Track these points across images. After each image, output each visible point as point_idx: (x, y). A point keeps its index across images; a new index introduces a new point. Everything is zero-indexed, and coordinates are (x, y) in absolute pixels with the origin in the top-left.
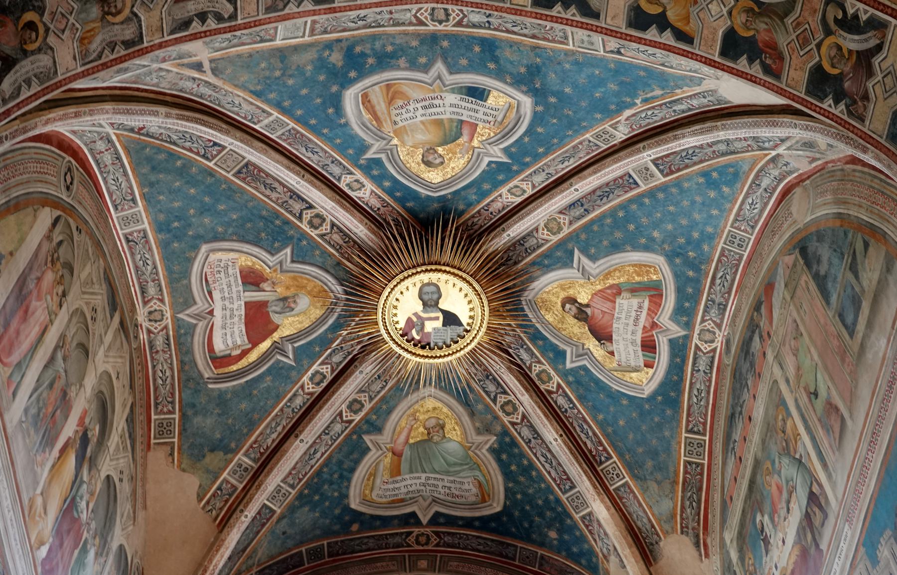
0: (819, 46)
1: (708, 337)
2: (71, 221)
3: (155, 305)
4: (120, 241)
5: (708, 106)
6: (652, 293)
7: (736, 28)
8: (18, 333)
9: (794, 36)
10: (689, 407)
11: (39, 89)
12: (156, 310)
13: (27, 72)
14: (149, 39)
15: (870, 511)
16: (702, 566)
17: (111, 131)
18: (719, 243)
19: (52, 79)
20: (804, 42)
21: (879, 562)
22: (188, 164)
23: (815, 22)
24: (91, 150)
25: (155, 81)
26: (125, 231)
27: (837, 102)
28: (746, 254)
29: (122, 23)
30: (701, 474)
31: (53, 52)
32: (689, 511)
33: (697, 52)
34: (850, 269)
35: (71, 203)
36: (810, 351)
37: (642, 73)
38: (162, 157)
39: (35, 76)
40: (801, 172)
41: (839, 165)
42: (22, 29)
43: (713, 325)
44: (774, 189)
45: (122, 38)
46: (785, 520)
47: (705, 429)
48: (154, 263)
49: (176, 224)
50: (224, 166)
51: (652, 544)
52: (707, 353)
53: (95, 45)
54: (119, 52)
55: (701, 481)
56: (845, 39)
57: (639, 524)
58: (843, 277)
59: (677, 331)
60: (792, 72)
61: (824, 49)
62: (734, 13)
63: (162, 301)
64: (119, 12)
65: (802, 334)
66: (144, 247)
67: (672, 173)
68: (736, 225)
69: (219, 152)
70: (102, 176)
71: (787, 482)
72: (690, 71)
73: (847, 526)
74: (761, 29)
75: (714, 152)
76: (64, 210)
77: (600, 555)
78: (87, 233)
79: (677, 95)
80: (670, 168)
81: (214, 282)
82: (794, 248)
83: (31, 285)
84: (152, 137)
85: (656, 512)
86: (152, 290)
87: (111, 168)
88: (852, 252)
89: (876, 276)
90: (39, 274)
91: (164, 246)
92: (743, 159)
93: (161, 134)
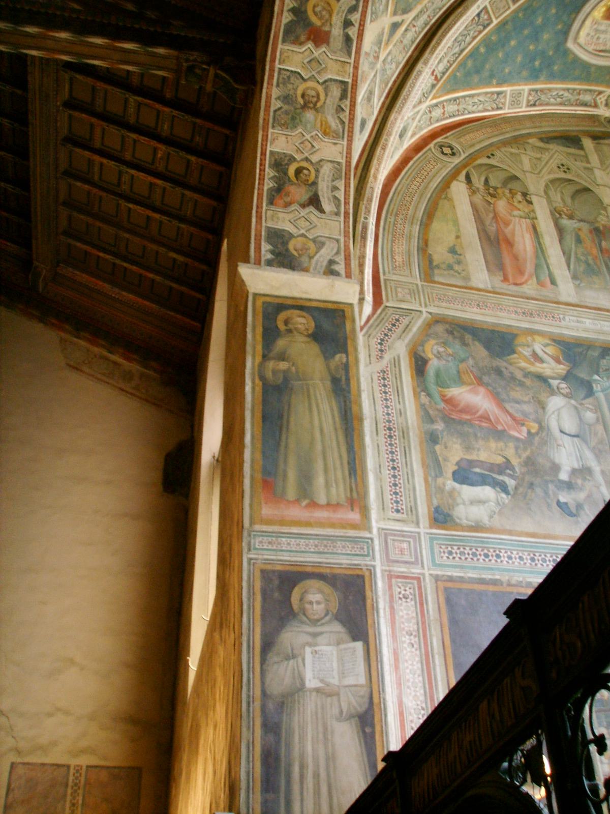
2: (479, 161)
3: (601, 99)
4: (530, 111)
8: (516, 258)
11: (343, 181)
12: (606, 100)
13: (328, 187)
14: (347, 76)
17: (428, 103)
19: (341, 169)
22: (486, 42)
24: (438, 121)
25: (394, 66)
26: (524, 105)
29: (327, 95)
31: (324, 160)
35: (466, 154)
38: (470, 63)
39: (333, 181)
42: (297, 179)
45: (337, 100)
48: (564, 90)
49: (537, 63)
50: (501, 12)
53: (334, 123)
54: (346, 106)
63: (600, 93)
64: (318, 96)
66: (545, 94)
69: (487, 12)
70: (466, 114)
76: (465, 166)
78: (498, 148)
81: (605, 45)
83: (492, 229)
84: (447, 70)
86: (587, 98)
87: (461, 107)
90: (491, 215)
91: (552, 77)
93: (448, 62)
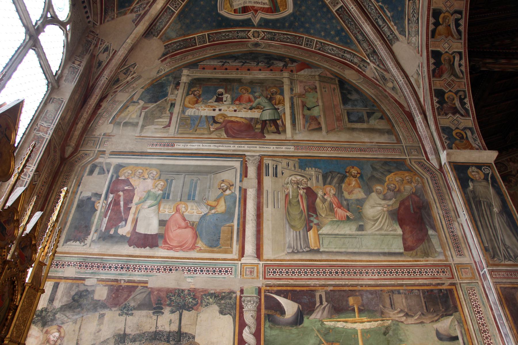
0: (450, 91)
1: (256, 35)
5: (385, 35)
6: (273, 8)
7: (443, 55)
9: (449, 80)
10: (220, 33)
15: (315, 158)
16: (157, 61)
18: (305, 35)
20: (449, 85)
21: (305, 170)
23: (456, 88)
27: (437, 102)
28: (303, 47)
30: (192, 46)
32: (175, 46)
33: (430, 40)
34: (367, 113)
36: (318, 99)
37: (400, 9)
40: (364, 73)
41: (387, 94)
43: (262, 36)
44: (345, 59)
46: (245, 108)
47: (212, 42)
51: (152, 33)
52: (248, 36)
55: (189, 47)
56: (457, 101)
57: (158, 24)
58: (361, 110)
59: (256, 21)
60: (438, 82)
61: (450, 93)
62: (447, 54)
65: (317, 92)
67: (339, 15)
68: (318, 43)
71: (259, 104)
72: (409, 32)
73: (293, 147)
74: (446, 66)
75: (356, 34)
77: (132, 8)
79: (390, 23)
80: (341, 14)
82: (336, 77)
85: (168, 31)
88: (373, 111)
89: (379, 127)
92: (357, 46)
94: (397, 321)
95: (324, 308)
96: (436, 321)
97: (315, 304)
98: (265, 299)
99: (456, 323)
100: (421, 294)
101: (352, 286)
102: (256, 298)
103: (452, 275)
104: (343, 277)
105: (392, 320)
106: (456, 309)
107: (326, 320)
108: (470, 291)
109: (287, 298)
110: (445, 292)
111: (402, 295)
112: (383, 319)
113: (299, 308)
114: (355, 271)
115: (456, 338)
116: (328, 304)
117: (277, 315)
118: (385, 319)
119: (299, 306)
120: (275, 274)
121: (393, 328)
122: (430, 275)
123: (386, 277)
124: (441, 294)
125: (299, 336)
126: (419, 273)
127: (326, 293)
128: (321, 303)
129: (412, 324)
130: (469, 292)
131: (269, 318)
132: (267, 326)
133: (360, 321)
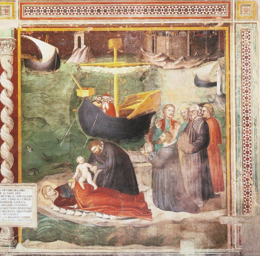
94: (156, 66)
95: (82, 52)
96: (198, 66)
97: (73, 48)
98: (21, 43)
99: (219, 68)
100: (188, 36)
101: (114, 27)
102: (13, 41)
103: (229, 13)
104: (106, 16)
105: (151, 65)
106: (222, 53)
107: (83, 65)
108: (245, 33)
109: (44, 41)
110: (216, 34)
111: (168, 38)
112: (142, 63)
113: (56, 51)
114: (119, 8)
115: (215, 84)
116: (86, 47)
117: (34, 60)
118: (144, 63)
119: (56, 49)
120: (31, 13)
121: (150, 73)
122: (203, 13)
123: (153, 16)
124: (210, 37)
125: (55, 81)
126: (191, 11)
127: (86, 34)
128: (79, 46)
129: (171, 69)
130: (243, 34)
131: (26, 63)
132: (24, 71)
133: (117, 65)
